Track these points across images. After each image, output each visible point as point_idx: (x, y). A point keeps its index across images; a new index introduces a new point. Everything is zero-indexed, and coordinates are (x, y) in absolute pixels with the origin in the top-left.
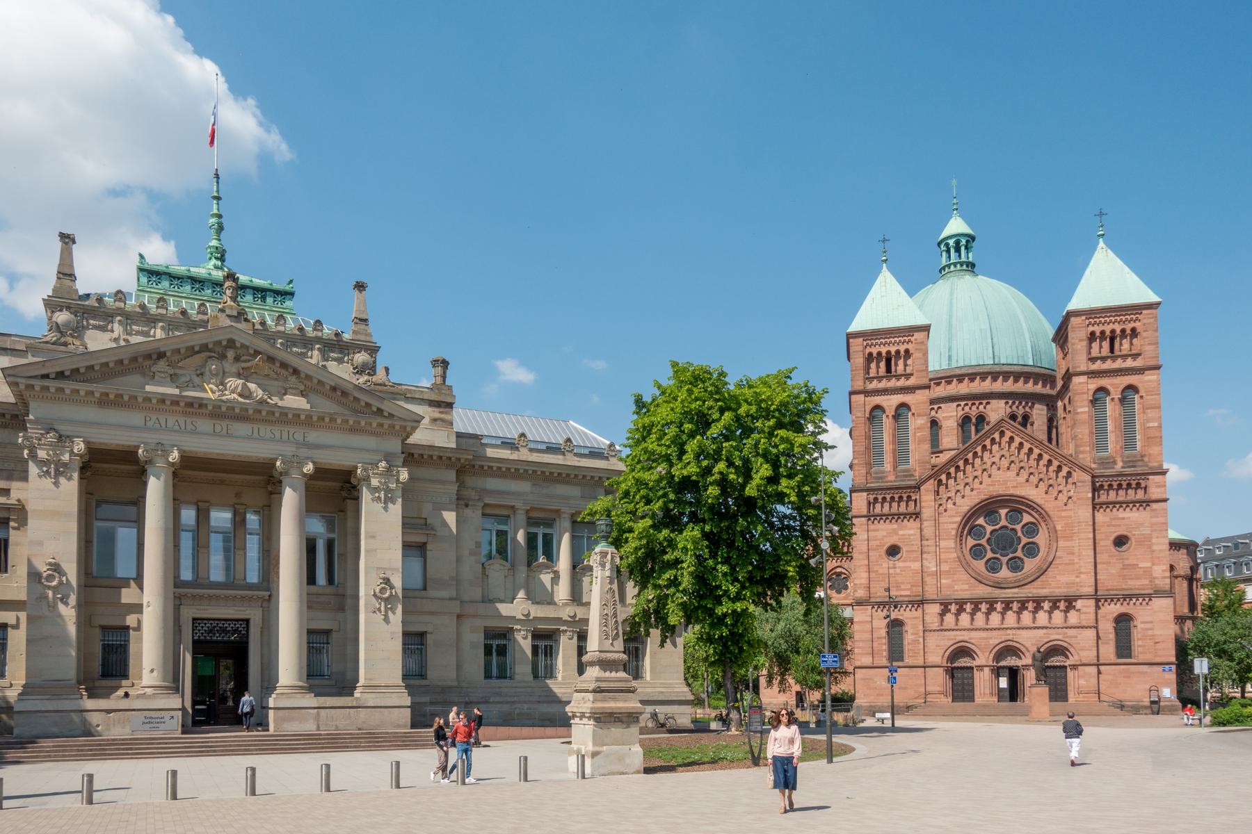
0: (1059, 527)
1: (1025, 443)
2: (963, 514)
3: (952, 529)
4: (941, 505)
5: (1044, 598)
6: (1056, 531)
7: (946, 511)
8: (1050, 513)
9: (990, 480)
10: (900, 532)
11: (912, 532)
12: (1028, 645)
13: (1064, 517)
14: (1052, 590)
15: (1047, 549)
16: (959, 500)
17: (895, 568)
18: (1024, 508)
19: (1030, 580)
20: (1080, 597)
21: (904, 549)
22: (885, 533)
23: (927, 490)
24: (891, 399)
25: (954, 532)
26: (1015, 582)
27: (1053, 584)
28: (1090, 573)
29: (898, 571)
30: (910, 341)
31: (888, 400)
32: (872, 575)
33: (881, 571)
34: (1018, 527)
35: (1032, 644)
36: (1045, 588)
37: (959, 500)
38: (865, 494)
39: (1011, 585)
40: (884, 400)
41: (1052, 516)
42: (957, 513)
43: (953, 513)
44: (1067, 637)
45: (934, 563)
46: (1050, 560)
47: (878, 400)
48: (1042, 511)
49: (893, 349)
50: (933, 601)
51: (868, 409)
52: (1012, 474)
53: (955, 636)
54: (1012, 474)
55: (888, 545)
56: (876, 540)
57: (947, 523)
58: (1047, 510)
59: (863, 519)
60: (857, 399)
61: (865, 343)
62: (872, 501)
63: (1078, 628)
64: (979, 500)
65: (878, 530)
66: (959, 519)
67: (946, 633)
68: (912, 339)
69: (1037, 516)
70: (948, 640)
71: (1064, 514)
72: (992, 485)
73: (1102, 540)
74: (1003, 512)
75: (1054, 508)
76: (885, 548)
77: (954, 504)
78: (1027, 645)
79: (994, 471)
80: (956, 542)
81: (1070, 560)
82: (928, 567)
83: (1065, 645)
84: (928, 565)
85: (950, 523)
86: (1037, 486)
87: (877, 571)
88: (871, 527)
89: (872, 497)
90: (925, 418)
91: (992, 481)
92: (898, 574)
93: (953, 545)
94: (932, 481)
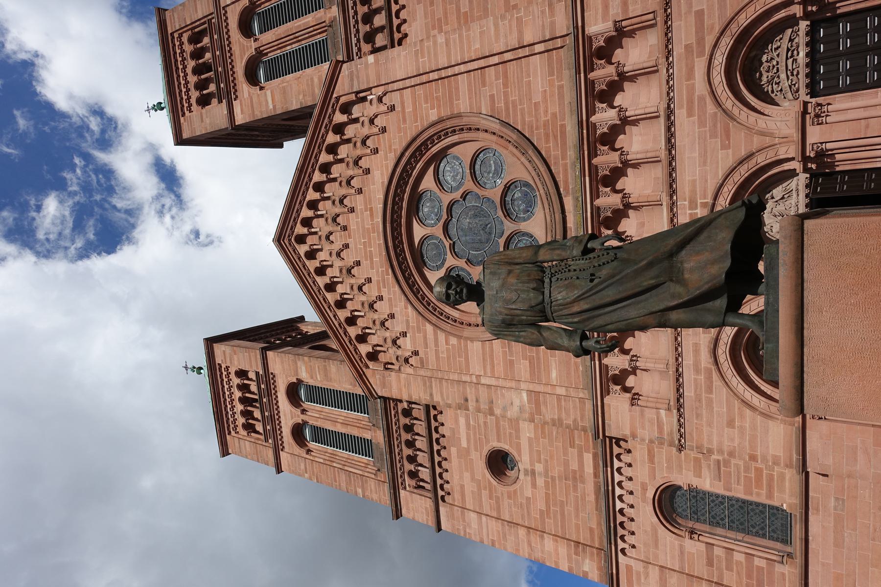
0: (433, 116)
1: (308, 198)
2: (421, 318)
3: (447, 343)
5: (586, 126)
6: (440, 121)
8: (409, 139)
9: (364, 263)
10: (464, 444)
11: (462, 421)
12: (725, 160)
13: (415, 109)
14: (567, 110)
15: (481, 135)
16: (397, 327)
17: (533, 472)
18: (408, 190)
19: (542, 169)
20: (578, 30)
21: (496, 445)
22: (467, 475)
23: (383, 385)
24: (284, 410)
25: (453, 341)
26: (551, 203)
27: (553, 108)
28: (519, 20)
29: (539, 468)
30: (227, 368)
31: (285, 415)
33: (541, 505)
34: (446, 199)
35: (724, 147)
36: (563, 126)
37: (397, 327)
38: (402, 493)
39: (558, 216)
40: (286, 423)
41: (414, 134)
42: (419, 331)
43: (420, 336)
44: (701, 41)
45: (513, 395)
46: (495, 126)
47: (286, 432)
48: (408, 154)
49: (238, 394)
50: (600, 413)
51: (297, 450)
52: (352, 220)
53: (697, 371)
54: (352, 220)
55: (488, 475)
56: (480, 495)
57: (437, 352)
58: (404, 144)
59: (443, 510)
60: (286, 463)
61: (233, 433)
62: (413, 483)
63: (668, 17)
64: (397, 288)
65: (462, 487)
66: (429, 328)
67: (689, 392)
68: (223, 366)
69: (419, 166)
70: (710, 389)
71: (409, 109)
72: (372, 259)
73: (458, 9)
74: (419, 232)
75: (399, 132)
76: (494, 482)
77: (404, 334)
78: (730, 162)
79: (350, 257)
80: (472, 340)
81: (497, 79)
82: (522, 409)
83: (727, 43)
84: (516, 409)
85: (436, 345)
86: (367, 171)
87: (541, 511)
88: (457, 495)
90: (299, 363)
91: (366, 260)
92: (546, 471)
93: (477, 345)
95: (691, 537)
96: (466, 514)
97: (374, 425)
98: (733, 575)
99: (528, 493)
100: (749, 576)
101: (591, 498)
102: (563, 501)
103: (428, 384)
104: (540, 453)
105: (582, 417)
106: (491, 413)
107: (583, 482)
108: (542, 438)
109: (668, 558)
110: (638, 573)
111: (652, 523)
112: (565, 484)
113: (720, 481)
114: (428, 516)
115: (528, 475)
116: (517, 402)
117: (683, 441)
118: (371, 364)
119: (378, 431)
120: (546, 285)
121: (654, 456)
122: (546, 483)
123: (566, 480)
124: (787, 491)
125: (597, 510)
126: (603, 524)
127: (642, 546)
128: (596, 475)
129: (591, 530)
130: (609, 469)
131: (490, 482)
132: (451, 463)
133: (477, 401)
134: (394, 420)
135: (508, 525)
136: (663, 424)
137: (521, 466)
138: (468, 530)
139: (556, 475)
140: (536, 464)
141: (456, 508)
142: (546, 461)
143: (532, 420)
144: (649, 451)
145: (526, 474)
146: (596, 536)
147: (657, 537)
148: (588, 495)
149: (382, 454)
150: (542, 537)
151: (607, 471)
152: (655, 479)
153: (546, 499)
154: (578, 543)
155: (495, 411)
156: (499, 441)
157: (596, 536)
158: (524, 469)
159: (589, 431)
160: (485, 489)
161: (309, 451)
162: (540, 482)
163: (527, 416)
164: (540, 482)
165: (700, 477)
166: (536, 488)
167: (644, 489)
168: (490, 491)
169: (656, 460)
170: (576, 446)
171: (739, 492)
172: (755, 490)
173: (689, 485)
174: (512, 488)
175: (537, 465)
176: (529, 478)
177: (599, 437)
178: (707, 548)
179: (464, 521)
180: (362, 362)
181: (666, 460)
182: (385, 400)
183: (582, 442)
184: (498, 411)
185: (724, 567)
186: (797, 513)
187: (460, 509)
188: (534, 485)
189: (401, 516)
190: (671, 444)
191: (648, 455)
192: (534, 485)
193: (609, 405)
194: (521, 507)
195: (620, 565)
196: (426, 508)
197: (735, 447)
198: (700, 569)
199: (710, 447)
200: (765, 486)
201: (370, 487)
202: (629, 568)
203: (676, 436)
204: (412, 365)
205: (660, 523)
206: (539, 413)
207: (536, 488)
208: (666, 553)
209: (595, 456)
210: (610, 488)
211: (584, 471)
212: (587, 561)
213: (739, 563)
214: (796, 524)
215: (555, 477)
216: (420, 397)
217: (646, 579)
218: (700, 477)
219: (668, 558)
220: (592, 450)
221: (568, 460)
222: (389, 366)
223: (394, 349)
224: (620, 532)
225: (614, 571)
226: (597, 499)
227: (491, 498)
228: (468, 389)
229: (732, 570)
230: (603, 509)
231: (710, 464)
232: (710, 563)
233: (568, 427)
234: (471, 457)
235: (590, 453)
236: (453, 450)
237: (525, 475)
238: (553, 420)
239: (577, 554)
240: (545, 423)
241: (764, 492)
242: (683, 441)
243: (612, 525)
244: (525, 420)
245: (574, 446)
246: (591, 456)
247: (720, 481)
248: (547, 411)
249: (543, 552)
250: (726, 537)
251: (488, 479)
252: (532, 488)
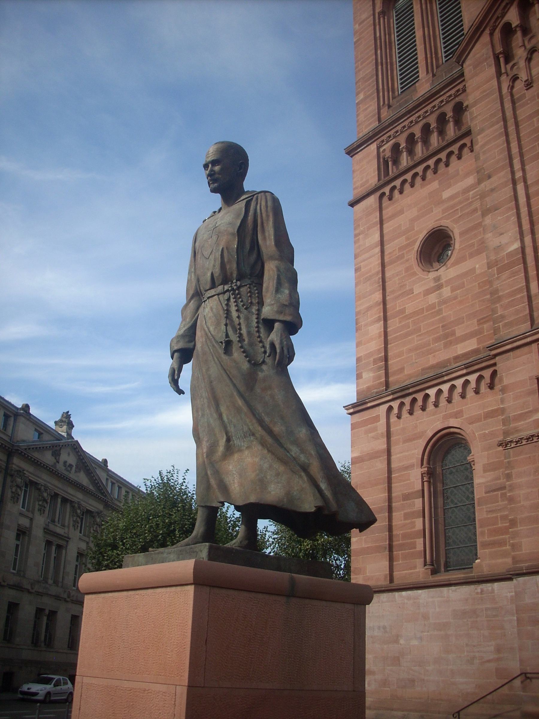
4: (515, 78)
7: (529, 85)
10: (446, 194)
17: (439, 287)
21: (456, 231)
29: (446, 292)
32: (393, 324)
33: (410, 307)
38: (374, 147)
55: (422, 236)
59: (372, 200)
62: (388, 154)
65: (401, 212)
76: (417, 246)
82: (499, 248)
87: (403, 311)
89: (388, 146)
92: (445, 302)
94: (485, 38)
95: (424, 473)
96: (376, 228)
97: (434, 75)
98: (401, 521)
99: (418, 289)
100: (405, 536)
101: (432, 360)
102: (420, 330)
103: (494, 119)
104: (463, 288)
105: (510, 324)
106: (485, 213)
107: (446, 346)
108: (479, 284)
109: (398, 455)
110: (375, 429)
111: (425, 431)
112: (439, 327)
113: (486, 493)
114: (360, 188)
115: (436, 282)
116: (504, 239)
117: (513, 445)
118: (497, 34)
119: (428, 84)
120: (220, 288)
121: (492, 417)
122: (433, 306)
123: (442, 326)
124: (493, 562)
125: (423, 370)
126: (411, 380)
127: (402, 426)
128: (457, 358)
129: (402, 370)
130: (464, 371)
131: (414, 242)
132: (421, 188)
133: (492, 190)
134: (444, 97)
135: (379, 279)
136: (525, 420)
137: (442, 271)
138: (361, 236)
139: (444, 314)
140: (449, 288)
141: (378, 214)
142: (455, 298)
143: (490, 266)
144: (496, 411)
145: (437, 279)
146: (399, 377)
147: (414, 439)
148: (434, 356)
149: (406, 102)
150: (378, 320)
151: (462, 369)
152: (470, 424)
153: (417, 311)
154: (386, 359)
155: (487, 217)
156: (462, 234)
157: (399, 377)
158: (440, 275)
159: (496, 337)
160: (407, 239)
161: (383, 13)
162: (433, 298)
163: (493, 258)
164: (433, 298)
165: (485, 471)
166: (424, 296)
167: (457, 415)
168: (408, 245)
169: (490, 420)
170: (481, 326)
171: (481, 514)
172: (486, 529)
173: (473, 461)
174: (417, 269)
175: (449, 288)
176: (432, 284)
177: (491, 350)
178: (418, 491)
179: (369, 228)
180: (495, 22)
181: (492, 431)
182: (462, 75)
183: (487, 332)
184: (488, 220)
185: (405, 511)
186: (474, 574)
187: (378, 219)
188: (427, 292)
189: (352, 157)
190: (506, 433)
191: (492, 410)
192: (427, 292)
193: (530, 352)
194: (401, 286)
195: (377, 408)
196: (367, 181)
197: (520, 502)
198: (398, 490)
199: (514, 476)
200: (492, 539)
201: (368, 107)
202: (377, 419)
203: (515, 437)
204: (513, 87)
205: (428, 440)
206: (501, 271)
207: (424, 296)
208: (402, 453)
209: (476, 351)
210: (446, 378)
211: (457, 344)
212: (371, 375)
213: (413, 525)
214: (464, 574)
215: (442, 314)
216: (476, 117)
217: (373, 438)
218: (485, 471)
219: (398, 455)
220: (481, 346)
221: (463, 322)
222: (502, 60)
223: (525, 55)
224: (407, 401)
225: (369, 405)
226: (433, 367)
227: (401, 249)
228: (502, 173)
229: (405, 519)
230: (426, 376)
231: (500, 479)
232: (406, 497)
233: (494, 311)
234: (434, 209)
235: (478, 344)
236: (435, 185)
237: (434, 279)
238: (496, 291)
239: (375, 362)
240: (490, 283)
241: (486, 539)
242: (513, 445)
243: (411, 390)
244: (488, 258)
245: (481, 324)
246: (475, 346)
247: (486, 493)
248: (505, 280)
249: (366, 325)
250: (436, 508)
251: (418, 238)
252: (424, 291)
